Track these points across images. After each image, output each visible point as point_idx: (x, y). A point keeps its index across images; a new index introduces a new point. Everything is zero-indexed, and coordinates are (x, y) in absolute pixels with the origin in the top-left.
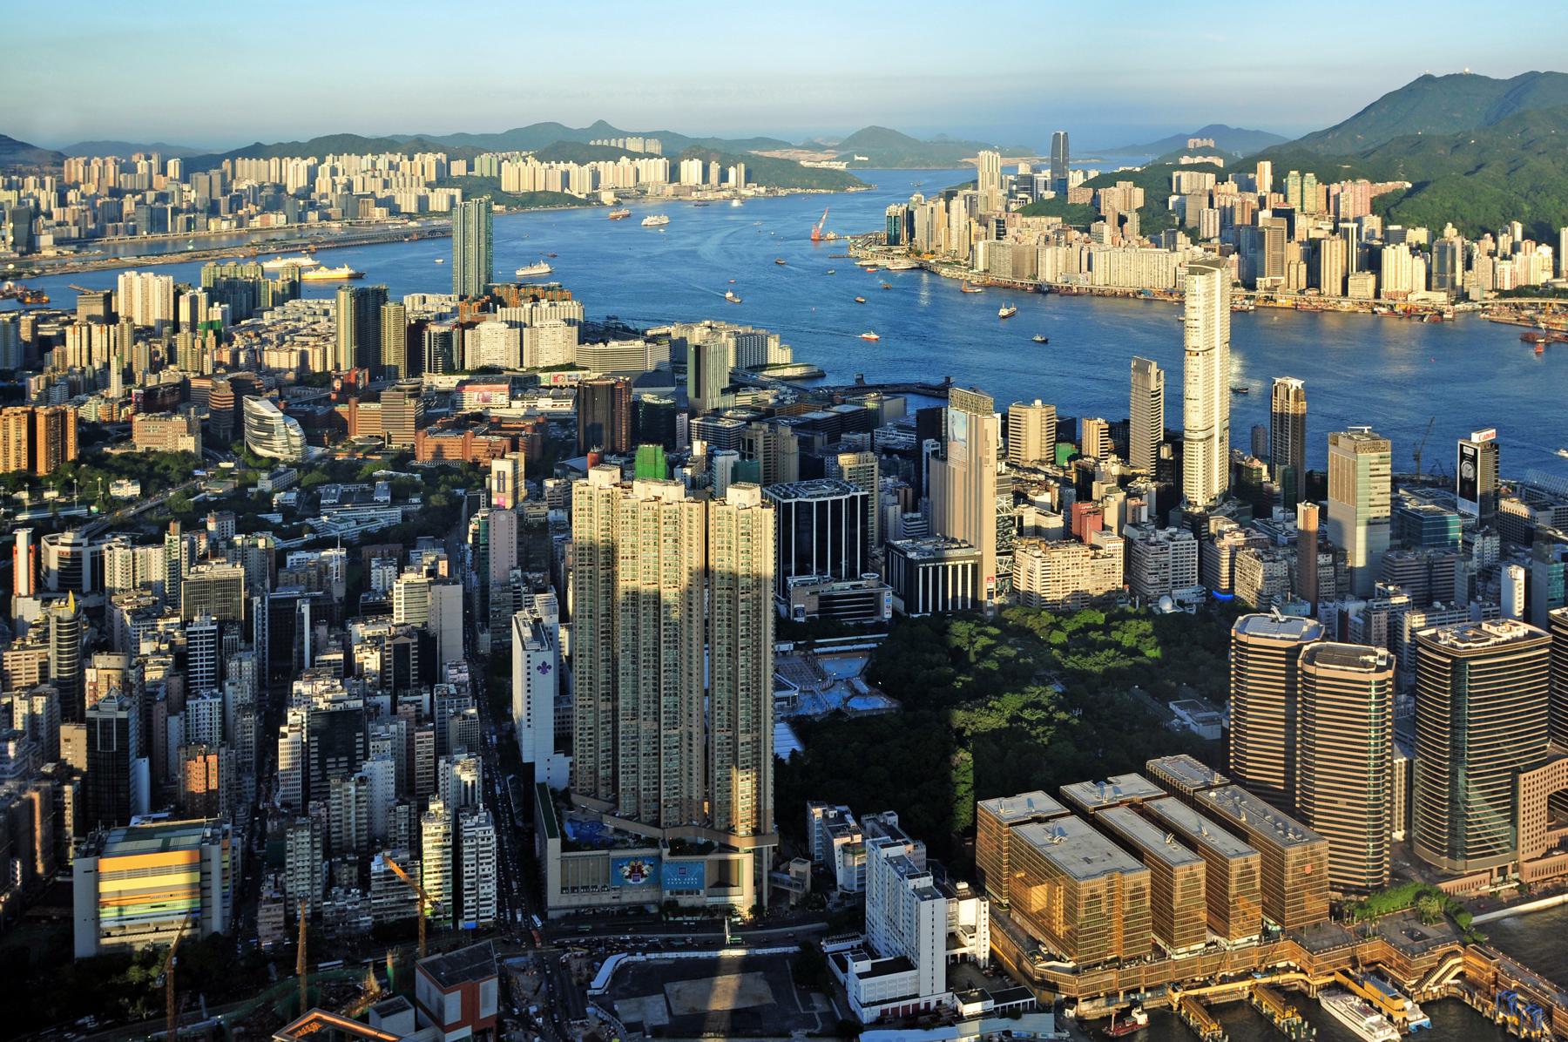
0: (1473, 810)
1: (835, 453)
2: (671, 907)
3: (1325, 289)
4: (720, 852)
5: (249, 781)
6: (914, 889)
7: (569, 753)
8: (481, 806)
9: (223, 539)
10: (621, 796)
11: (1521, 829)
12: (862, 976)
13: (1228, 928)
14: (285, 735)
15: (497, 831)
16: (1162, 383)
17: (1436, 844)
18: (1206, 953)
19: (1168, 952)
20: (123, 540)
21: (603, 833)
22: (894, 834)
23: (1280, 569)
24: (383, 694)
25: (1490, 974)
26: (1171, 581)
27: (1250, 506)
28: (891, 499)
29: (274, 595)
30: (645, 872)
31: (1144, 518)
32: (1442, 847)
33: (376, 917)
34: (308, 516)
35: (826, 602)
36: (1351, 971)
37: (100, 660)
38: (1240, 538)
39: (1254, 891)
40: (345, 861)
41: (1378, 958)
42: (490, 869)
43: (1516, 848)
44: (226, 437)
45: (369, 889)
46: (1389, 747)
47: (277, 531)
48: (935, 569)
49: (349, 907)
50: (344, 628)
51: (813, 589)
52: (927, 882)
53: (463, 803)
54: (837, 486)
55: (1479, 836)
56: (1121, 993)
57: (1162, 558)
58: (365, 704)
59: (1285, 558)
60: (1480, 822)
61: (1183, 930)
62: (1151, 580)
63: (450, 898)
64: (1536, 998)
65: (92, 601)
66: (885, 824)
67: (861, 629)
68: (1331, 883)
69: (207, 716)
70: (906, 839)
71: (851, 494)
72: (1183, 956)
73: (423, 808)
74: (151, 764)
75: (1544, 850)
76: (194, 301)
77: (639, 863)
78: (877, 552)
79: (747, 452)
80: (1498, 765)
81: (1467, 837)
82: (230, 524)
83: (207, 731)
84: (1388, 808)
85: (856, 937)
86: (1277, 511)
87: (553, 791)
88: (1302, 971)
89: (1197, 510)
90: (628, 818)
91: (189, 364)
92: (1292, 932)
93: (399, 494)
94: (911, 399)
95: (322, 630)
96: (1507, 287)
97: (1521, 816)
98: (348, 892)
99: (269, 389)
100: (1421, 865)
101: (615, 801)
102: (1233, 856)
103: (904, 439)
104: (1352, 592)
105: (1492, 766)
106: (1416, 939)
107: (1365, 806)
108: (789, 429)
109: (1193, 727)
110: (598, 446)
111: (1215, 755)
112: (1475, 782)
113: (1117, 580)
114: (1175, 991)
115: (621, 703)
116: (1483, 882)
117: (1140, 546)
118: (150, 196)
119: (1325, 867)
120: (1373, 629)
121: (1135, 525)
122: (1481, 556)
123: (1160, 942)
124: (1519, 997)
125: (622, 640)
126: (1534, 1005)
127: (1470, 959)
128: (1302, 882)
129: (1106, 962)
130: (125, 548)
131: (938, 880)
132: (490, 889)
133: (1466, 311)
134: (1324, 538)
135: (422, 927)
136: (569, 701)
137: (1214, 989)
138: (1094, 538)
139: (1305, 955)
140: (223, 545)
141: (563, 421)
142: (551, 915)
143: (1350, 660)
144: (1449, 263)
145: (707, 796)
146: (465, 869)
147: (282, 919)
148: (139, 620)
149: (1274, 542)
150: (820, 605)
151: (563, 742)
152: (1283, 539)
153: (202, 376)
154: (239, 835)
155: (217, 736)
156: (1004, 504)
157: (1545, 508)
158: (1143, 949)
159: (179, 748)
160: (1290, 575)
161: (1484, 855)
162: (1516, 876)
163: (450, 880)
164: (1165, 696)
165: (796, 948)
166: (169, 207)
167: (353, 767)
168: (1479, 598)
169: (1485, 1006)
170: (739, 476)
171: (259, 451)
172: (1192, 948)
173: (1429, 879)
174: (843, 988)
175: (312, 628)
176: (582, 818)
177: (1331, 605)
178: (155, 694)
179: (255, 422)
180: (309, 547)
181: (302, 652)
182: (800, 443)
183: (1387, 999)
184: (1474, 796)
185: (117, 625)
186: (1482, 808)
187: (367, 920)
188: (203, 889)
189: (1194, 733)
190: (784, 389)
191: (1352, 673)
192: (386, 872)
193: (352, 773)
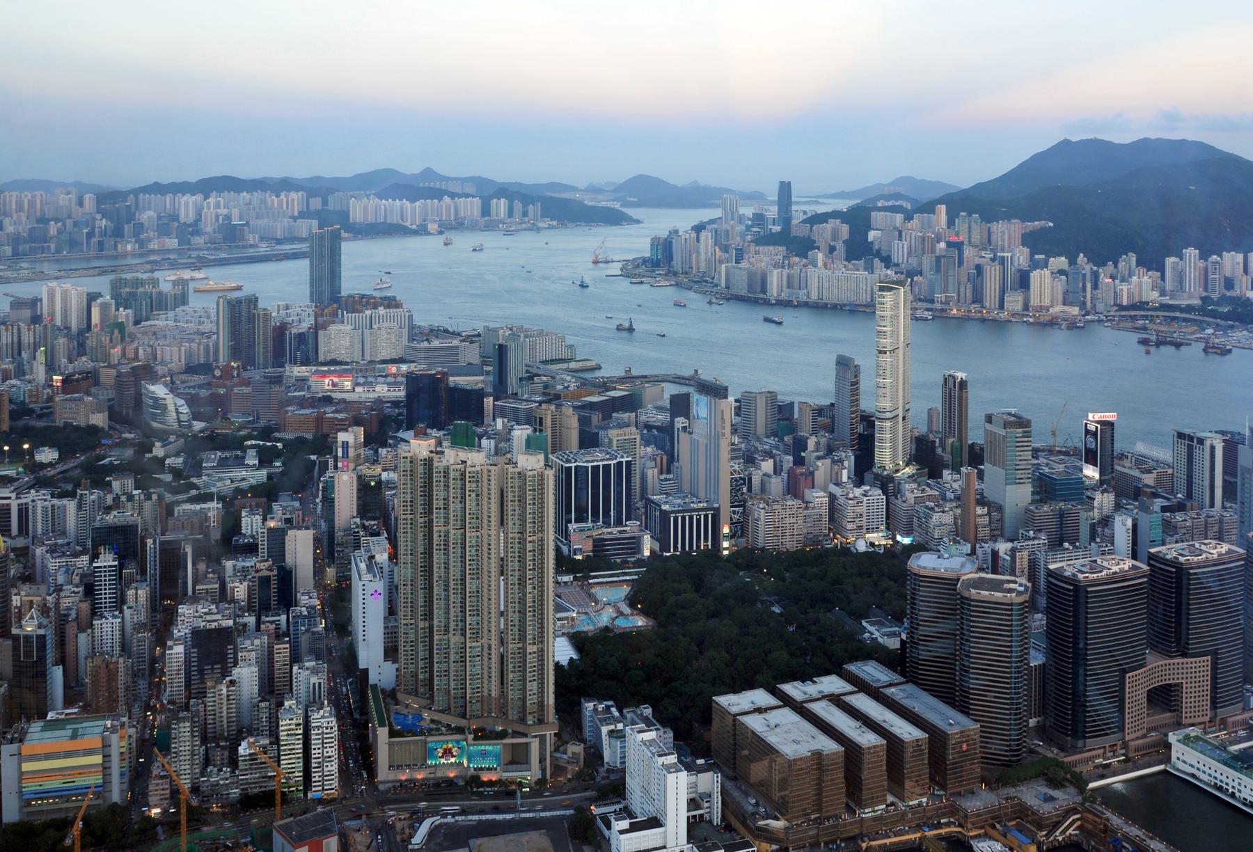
0: (1090, 701)
1: (606, 428)
2: (475, 781)
4: (513, 737)
5: (142, 684)
6: (663, 765)
7: (395, 661)
8: (326, 702)
9: (124, 494)
10: (436, 694)
12: (622, 832)
14: (171, 648)
15: (338, 720)
20: (44, 495)
21: (422, 723)
22: (649, 724)
24: (250, 615)
25: (1102, 827)
26: (865, 527)
28: (650, 464)
29: (164, 538)
30: (455, 754)
31: (845, 479)
33: (242, 790)
34: (192, 476)
35: (599, 544)
37: (25, 589)
39: (923, 764)
40: (218, 746)
42: (332, 751)
43: (1123, 730)
44: (128, 414)
45: (237, 767)
47: (167, 486)
48: (683, 518)
49: (222, 782)
50: (219, 563)
51: (589, 533)
52: (672, 759)
53: (312, 700)
54: (608, 453)
55: (1094, 721)
57: (858, 510)
58: (235, 623)
62: (850, 526)
63: (301, 774)
65: (20, 542)
66: (642, 714)
67: (624, 564)
69: (110, 633)
70: (658, 726)
71: (618, 460)
73: (281, 704)
74: (64, 671)
76: (104, 306)
77: (450, 746)
78: (640, 504)
79: (538, 427)
82: (130, 482)
83: (109, 645)
85: (619, 802)
86: (947, 474)
87: (383, 691)
88: (960, 825)
89: (885, 473)
90: (442, 712)
91: (99, 355)
93: (265, 458)
94: (663, 385)
95: (202, 567)
96: (1125, 303)
98: (220, 770)
99: (164, 376)
101: (432, 698)
103: (660, 418)
104: (1002, 536)
108: (571, 409)
109: (880, 640)
110: (423, 423)
112: (1091, 680)
115: (436, 623)
116: (1098, 757)
117: (841, 501)
118: (69, 222)
119: (978, 745)
121: (837, 484)
122: (1101, 508)
123: (852, 805)
125: (438, 572)
130: (45, 500)
131: (683, 758)
132: (332, 767)
134: (982, 494)
135: (278, 797)
136: (396, 620)
140: (123, 498)
141: (396, 404)
142: (381, 787)
143: (996, 586)
145: (503, 694)
146: (313, 752)
147: (168, 791)
148: (55, 558)
149: (944, 498)
150: (594, 546)
151: (391, 652)
152: (950, 495)
153: (110, 366)
154: (134, 726)
155: (117, 649)
156: (737, 467)
157: (1149, 472)
159: (86, 658)
160: (955, 523)
162: (1123, 751)
163: (301, 760)
164: (859, 615)
165: (572, 812)
166: (85, 231)
167: (225, 672)
170: (531, 445)
171: (155, 425)
172: (876, 808)
174: (608, 841)
175: (194, 564)
176: (405, 711)
177: (986, 545)
178: (67, 615)
179: (151, 402)
180: (193, 500)
181: (185, 583)
182: (579, 420)
185: (38, 561)
186: (1098, 700)
187: (235, 792)
188: (105, 768)
190: (569, 378)
192: (250, 755)
193: (224, 677)
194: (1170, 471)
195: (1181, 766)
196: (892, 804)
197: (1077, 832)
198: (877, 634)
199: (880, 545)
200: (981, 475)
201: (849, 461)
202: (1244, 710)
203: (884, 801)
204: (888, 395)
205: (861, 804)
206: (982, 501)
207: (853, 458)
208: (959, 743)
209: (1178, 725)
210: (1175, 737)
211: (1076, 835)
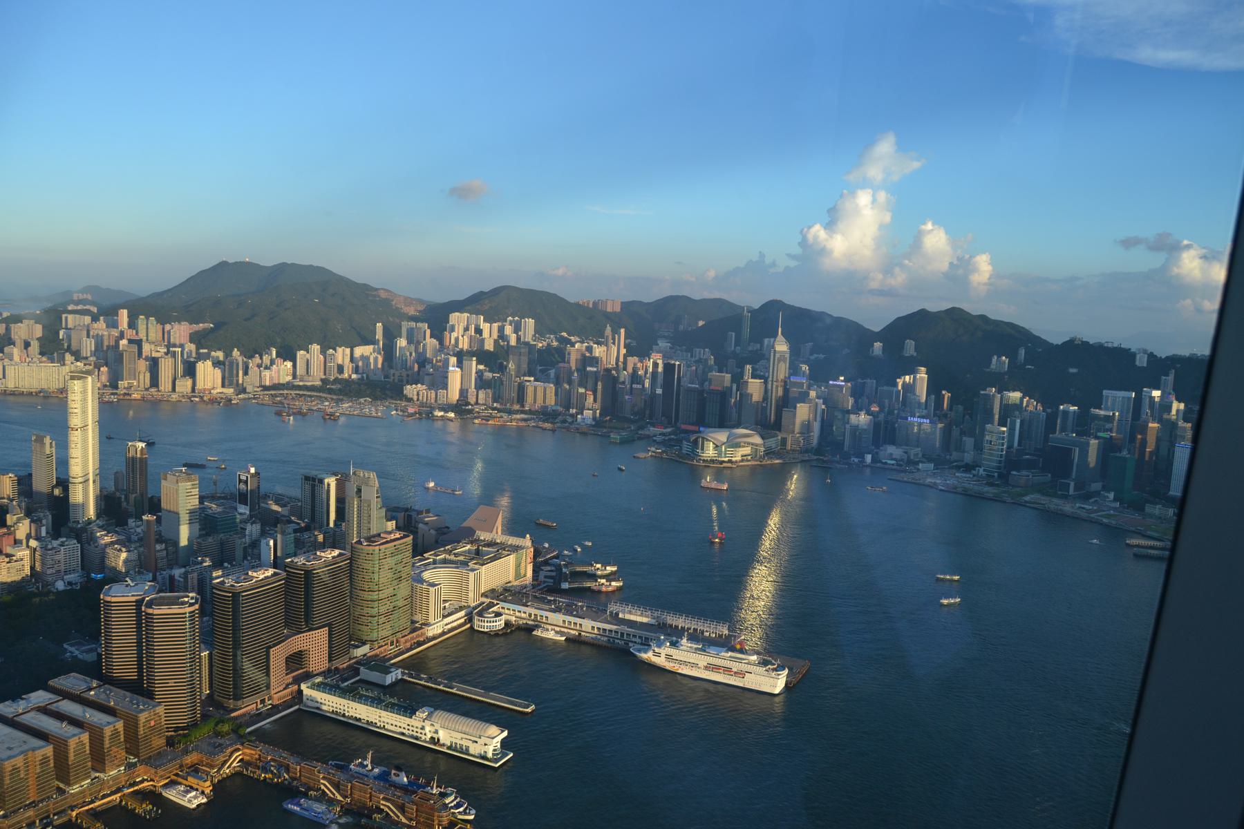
0: (246, 672)
3: (162, 388)
11: (272, 677)
16: (54, 449)
17: (227, 695)
18: (91, 784)
19: (67, 790)
23: (134, 556)
27: (114, 521)
31: (44, 534)
32: (230, 695)
38: (107, 539)
41: (196, 762)
43: (268, 687)
46: (197, 647)
56: (38, 821)
57: (57, 558)
59: (136, 548)
60: (250, 678)
64: (281, 762)
68: (167, 728)
72: (78, 790)
75: (284, 686)
80: (259, 646)
81: (243, 687)
84: (198, 681)
86: (131, 522)
89: (79, 526)
92: (143, 760)
97: (272, 670)
100: (219, 706)
102: (105, 726)
104: (177, 564)
105: (255, 648)
106: (217, 747)
107: (185, 682)
109: (80, 656)
111: (96, 670)
112: (246, 658)
113: (27, 571)
114: (73, 811)
119: (163, 720)
120: (189, 583)
122: (251, 535)
123: (62, 785)
124: (272, 763)
126: (280, 766)
127: (248, 751)
128: (149, 731)
129: (26, 806)
133: (244, 399)
138: (9, 550)
139: (153, 771)
144: (235, 372)
149: (129, 540)
152: (134, 538)
158: (50, 792)
161: (252, 695)
162: (270, 702)
168: (249, 558)
169: (254, 773)
172: (83, 784)
177: (164, 572)
183: (201, 783)
184: (247, 665)
186: (251, 670)
189: (80, 660)
191: (175, 610)
194: (300, 504)
195: (310, 703)
196: (96, 778)
197: (239, 764)
198: (77, 652)
199: (76, 584)
200: (159, 520)
201: (47, 519)
202: (350, 659)
204: (80, 464)
205: (69, 784)
206: (160, 540)
207: (50, 516)
208: (149, 721)
209: (307, 676)
210: (305, 685)
211: (238, 766)
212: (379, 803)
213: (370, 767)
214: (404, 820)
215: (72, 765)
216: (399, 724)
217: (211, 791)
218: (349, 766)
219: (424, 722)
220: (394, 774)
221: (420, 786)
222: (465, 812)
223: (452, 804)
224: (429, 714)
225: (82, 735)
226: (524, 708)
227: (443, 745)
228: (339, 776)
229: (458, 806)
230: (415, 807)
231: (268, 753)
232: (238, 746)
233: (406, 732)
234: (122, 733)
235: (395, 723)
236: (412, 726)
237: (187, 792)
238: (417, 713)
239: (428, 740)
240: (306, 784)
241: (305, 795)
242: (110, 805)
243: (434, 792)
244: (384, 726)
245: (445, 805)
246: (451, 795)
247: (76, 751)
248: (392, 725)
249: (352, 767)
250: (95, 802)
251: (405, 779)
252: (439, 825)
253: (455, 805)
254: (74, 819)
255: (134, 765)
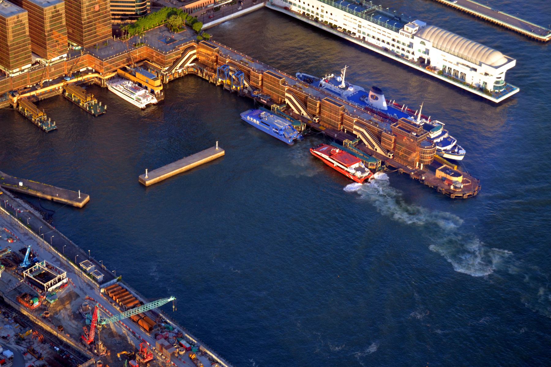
13: (46, 52)
18: (32, 70)
19: (7, 73)
36: (127, 67)
39: (62, 27)
41: (145, 57)
61: (15, 57)
68: (113, 15)
88: (96, 72)
92: (87, 49)
102: (46, 6)
106: (168, 43)
114: (14, 96)
124: (231, 68)
126: (240, 71)
137: (39, 91)
139: (98, 62)
172: (23, 68)
173: (175, 5)
183: (151, 81)
196: (37, 63)
197: (193, 64)
203: (27, 60)
205: (8, 67)
208: (93, 4)
211: (193, 67)
212: (352, 127)
213: (343, 85)
214: (379, 151)
215: (11, 46)
216: (382, 38)
217: (161, 91)
218: (319, 80)
219: (413, 38)
220: (372, 96)
221: (401, 114)
222: (453, 152)
223: (438, 140)
224: (419, 30)
225: (20, 14)
226: (541, 35)
227: (434, 69)
228: (308, 91)
229: (445, 143)
230: (393, 138)
231: (226, 55)
232: (192, 44)
233: (390, 47)
234: (64, 15)
235: (377, 36)
236: (398, 42)
237: (135, 89)
238: (405, 27)
239: (416, 60)
240: (268, 95)
241: (268, 108)
242: (53, 94)
243: (418, 123)
244: (364, 38)
245: (430, 140)
246: (438, 129)
247: (16, 31)
248: (373, 37)
249: (322, 82)
250: (37, 89)
251: (385, 104)
252: (420, 162)
253: (441, 141)
254: (15, 105)
255: (78, 53)
